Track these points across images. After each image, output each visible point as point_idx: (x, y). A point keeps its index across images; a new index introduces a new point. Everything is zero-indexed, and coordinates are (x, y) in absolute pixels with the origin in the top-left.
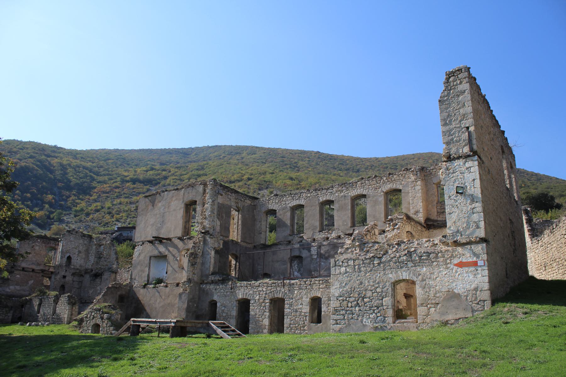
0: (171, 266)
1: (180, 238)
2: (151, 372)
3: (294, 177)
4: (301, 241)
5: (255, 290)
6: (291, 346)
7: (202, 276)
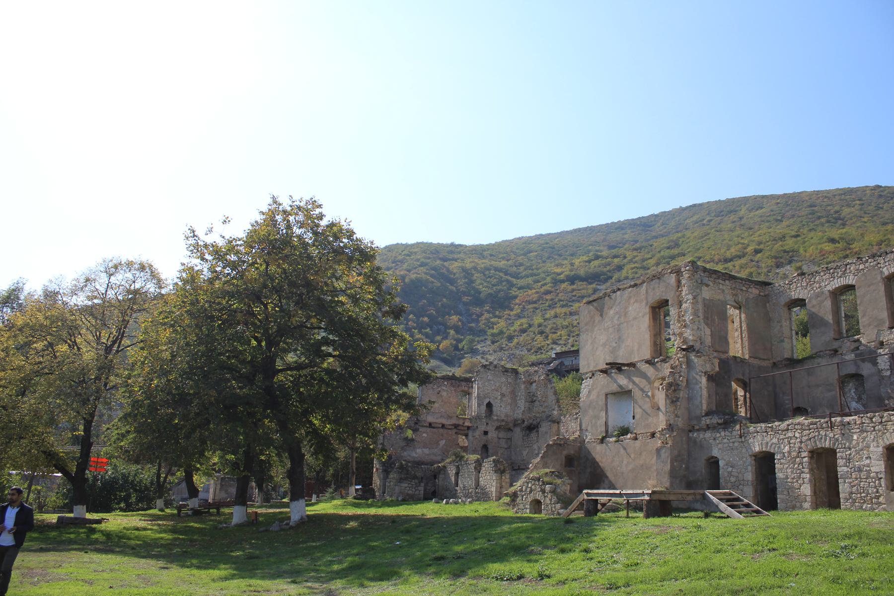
0: (640, 407)
1: (648, 362)
2: (614, 570)
3: (836, 237)
4: (857, 348)
5: (782, 436)
6: (846, 531)
7: (690, 419)
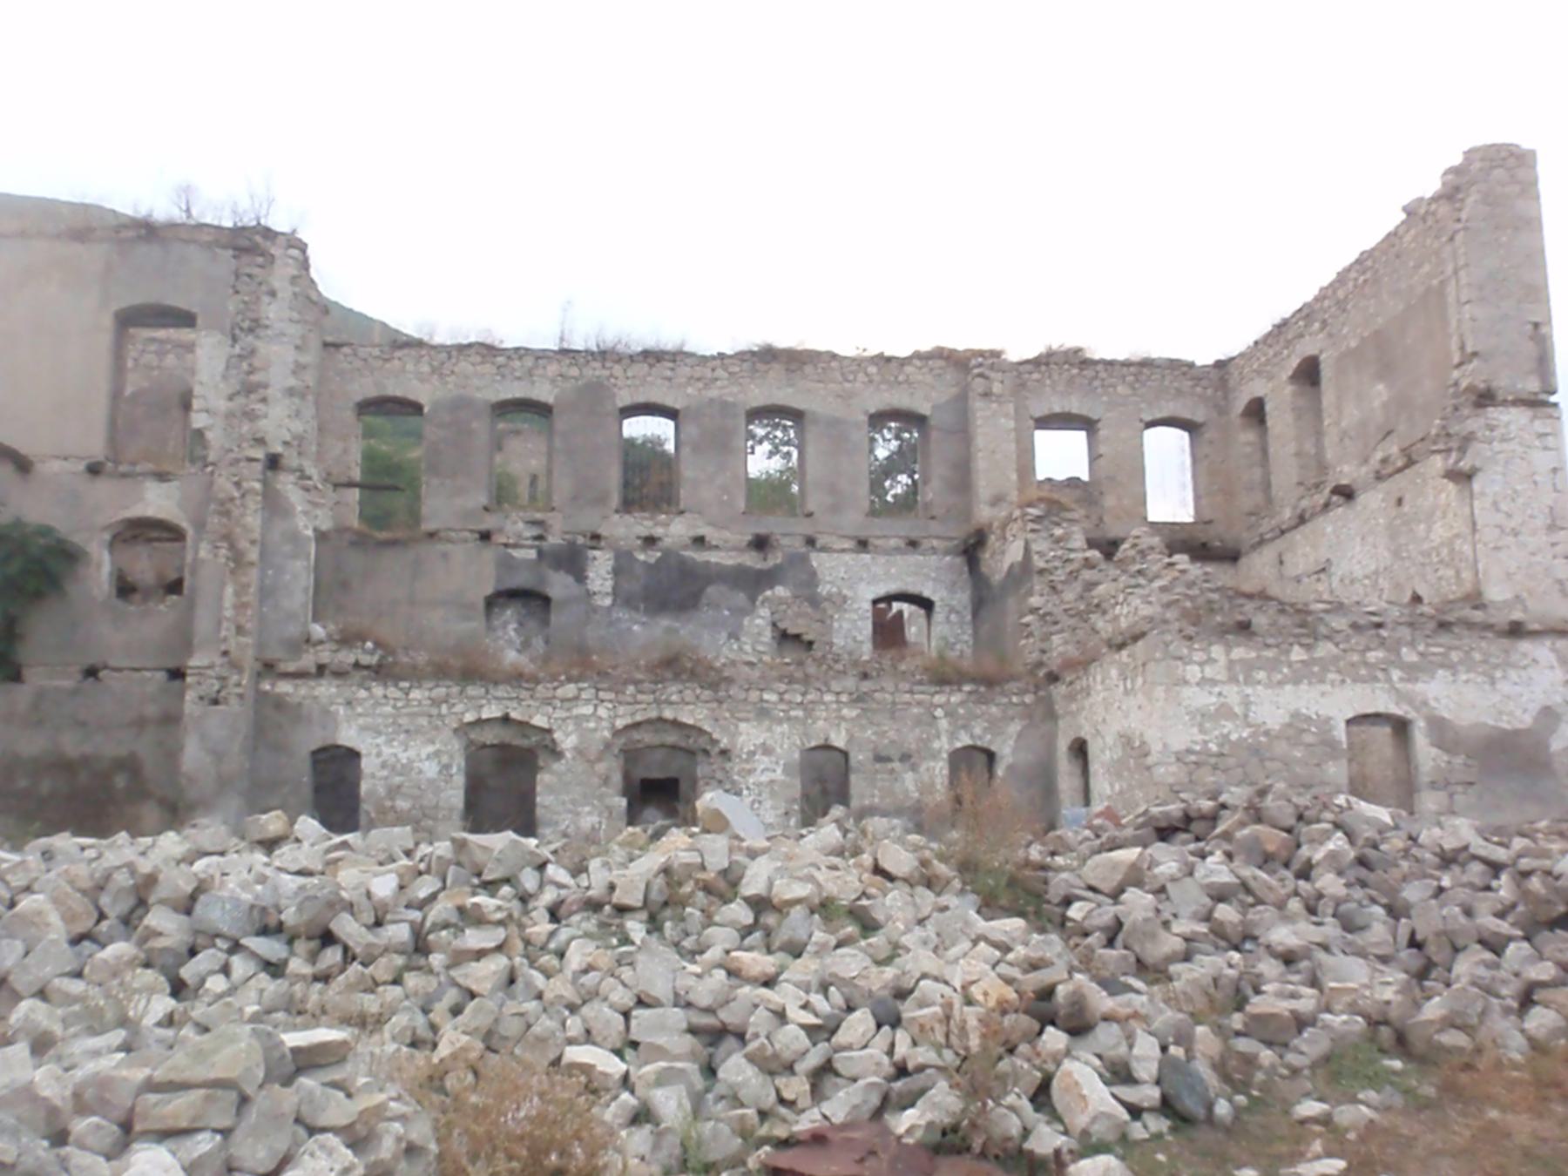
4: (540, 538)
